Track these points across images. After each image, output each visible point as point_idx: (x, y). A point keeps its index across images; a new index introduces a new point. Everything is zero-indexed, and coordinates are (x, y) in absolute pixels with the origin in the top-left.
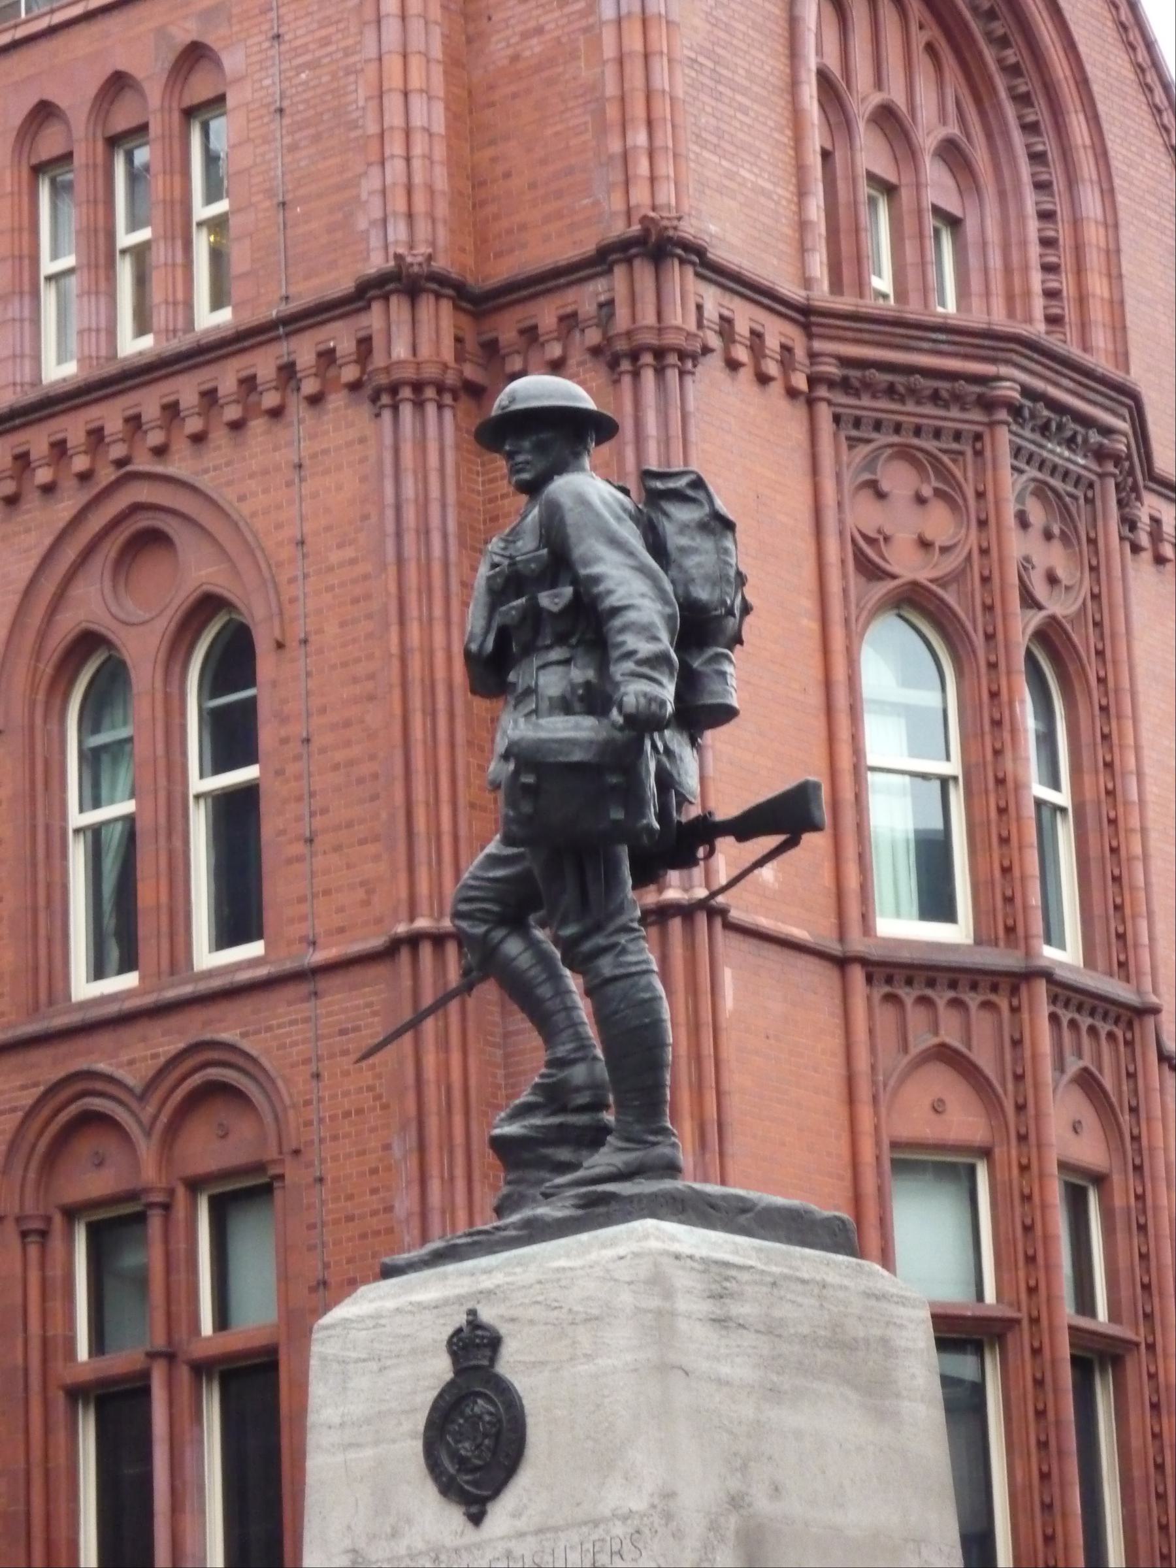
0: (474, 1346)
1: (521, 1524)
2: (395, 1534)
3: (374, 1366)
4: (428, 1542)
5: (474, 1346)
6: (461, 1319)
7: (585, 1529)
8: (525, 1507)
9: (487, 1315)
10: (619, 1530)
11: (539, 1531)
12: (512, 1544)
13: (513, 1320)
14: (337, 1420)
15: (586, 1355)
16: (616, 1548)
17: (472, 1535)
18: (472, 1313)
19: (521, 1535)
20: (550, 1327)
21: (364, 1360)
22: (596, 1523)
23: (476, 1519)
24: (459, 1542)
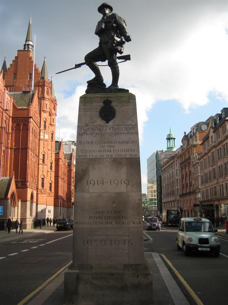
2: (93, 123)
3: (90, 103)
7: (125, 126)
8: (115, 122)
10: (130, 126)
11: (117, 125)
12: (113, 126)
14: (84, 108)
16: (130, 128)
17: (107, 124)
19: (114, 125)
22: (127, 125)
23: (108, 123)
24: (104, 125)
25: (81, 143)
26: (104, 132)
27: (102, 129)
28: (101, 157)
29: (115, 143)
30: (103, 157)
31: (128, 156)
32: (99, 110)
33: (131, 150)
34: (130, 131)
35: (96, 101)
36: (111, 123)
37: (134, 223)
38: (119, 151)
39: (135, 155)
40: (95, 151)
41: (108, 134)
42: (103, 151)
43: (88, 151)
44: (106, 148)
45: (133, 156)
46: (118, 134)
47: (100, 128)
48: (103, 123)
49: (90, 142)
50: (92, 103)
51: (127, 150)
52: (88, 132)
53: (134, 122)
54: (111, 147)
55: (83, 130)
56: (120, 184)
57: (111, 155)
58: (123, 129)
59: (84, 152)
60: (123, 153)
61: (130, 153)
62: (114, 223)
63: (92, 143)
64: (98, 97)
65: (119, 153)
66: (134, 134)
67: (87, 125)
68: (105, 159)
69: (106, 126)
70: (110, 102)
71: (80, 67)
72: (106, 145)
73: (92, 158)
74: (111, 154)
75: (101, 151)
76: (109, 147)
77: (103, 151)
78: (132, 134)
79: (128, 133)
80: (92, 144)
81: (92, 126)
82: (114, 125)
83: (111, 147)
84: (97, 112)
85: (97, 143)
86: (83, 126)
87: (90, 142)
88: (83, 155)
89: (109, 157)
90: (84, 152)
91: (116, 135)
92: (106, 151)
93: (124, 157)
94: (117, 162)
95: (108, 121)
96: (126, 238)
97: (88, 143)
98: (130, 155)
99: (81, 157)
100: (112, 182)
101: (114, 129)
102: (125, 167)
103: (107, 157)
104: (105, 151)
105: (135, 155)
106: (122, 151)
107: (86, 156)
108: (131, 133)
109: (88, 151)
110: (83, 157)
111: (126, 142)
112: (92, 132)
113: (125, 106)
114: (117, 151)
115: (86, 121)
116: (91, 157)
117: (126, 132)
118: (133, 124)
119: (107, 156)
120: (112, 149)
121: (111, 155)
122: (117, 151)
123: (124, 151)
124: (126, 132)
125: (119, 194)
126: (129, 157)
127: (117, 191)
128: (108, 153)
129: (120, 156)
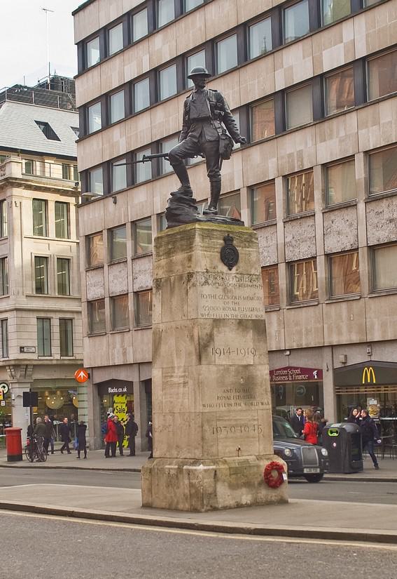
0: (228, 240)
9: (231, 235)
10: (254, 277)
23: (230, 270)
32: (219, 250)
34: (255, 283)
36: (234, 269)
37: (262, 404)
44: (231, 305)
48: (225, 269)
56: (247, 353)
59: (207, 309)
60: (249, 313)
61: (255, 313)
62: (242, 404)
63: (215, 297)
64: (217, 230)
67: (207, 272)
70: (232, 240)
72: (231, 301)
74: (236, 313)
82: (237, 274)
94: (242, 324)
96: (256, 423)
98: (256, 317)
100: (239, 352)
116: (215, 317)
117: (249, 283)
125: (246, 367)
127: (245, 363)
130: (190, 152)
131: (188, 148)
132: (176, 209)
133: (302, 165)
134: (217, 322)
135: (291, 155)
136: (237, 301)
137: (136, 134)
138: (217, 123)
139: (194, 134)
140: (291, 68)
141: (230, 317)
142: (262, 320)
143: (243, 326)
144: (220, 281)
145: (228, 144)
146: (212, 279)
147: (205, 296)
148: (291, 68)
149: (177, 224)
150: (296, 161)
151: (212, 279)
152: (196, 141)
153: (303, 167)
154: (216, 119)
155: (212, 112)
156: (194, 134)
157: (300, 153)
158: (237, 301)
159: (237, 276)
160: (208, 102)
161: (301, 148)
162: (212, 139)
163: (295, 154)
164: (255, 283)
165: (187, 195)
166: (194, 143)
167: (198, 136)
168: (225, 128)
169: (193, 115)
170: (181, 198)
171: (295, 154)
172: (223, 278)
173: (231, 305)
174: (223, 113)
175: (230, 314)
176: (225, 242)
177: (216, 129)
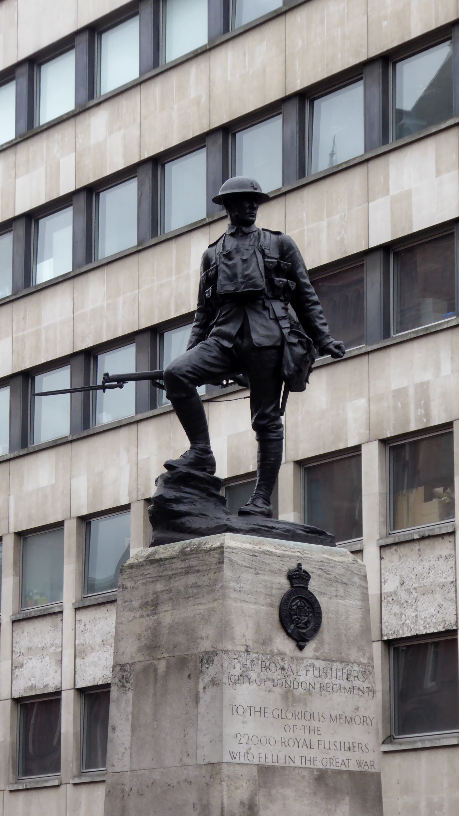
0: (298, 577)
1: (317, 654)
3: (253, 571)
4: (279, 651)
5: (298, 577)
6: (294, 566)
10: (356, 668)
12: (314, 661)
13: (313, 573)
15: (342, 596)
16: (356, 675)
17: (298, 654)
18: (299, 565)
20: (326, 580)
21: (249, 567)
23: (301, 648)
25: (235, 708)
26: (291, 679)
27: (286, 666)
28: (287, 765)
29: (322, 719)
30: (292, 764)
31: (353, 767)
33: (360, 746)
35: (267, 568)
38: (333, 747)
39: (369, 764)
40: (272, 742)
41: (304, 685)
42: (291, 743)
43: (255, 739)
44: (301, 735)
45: (366, 768)
46: (329, 690)
47: (282, 664)
49: (258, 709)
50: (257, 574)
51: (351, 746)
52: (253, 675)
53: (364, 654)
54: (312, 732)
55: (238, 666)
57: (312, 760)
58: (339, 674)
59: (244, 740)
60: (341, 756)
64: (271, 554)
65: (332, 753)
66: (366, 694)
68: (297, 771)
69: (297, 659)
71: (121, 387)
72: (300, 723)
73: (264, 763)
74: (312, 753)
75: (286, 743)
76: (307, 731)
77: (291, 743)
78: (360, 692)
79: (352, 690)
80: (263, 715)
81: (263, 654)
82: (318, 658)
83: (312, 732)
84: (271, 605)
85: (276, 715)
86: (239, 652)
87: (258, 709)
88: (242, 754)
89: (308, 765)
90: (244, 740)
91: (323, 692)
92: (300, 745)
93: (343, 768)
95: (302, 644)
97: (253, 712)
98: (359, 764)
99: (237, 760)
101: (317, 673)
102: (347, 800)
103: (304, 765)
104: (296, 743)
105: (369, 764)
106: (339, 748)
107: (250, 757)
108: (359, 689)
109: (255, 739)
110: (242, 760)
111: (349, 719)
112: (263, 676)
113: (343, 598)
114: (327, 746)
115: (244, 636)
116: (262, 761)
117: (348, 685)
118: (362, 662)
119: (304, 761)
120: (315, 739)
121: (312, 760)
122: (327, 746)
123: (343, 749)
124: (348, 685)
126: (357, 769)
128: (305, 751)
129: (334, 763)
130: (213, 369)
131: (210, 360)
132: (177, 501)
133: (427, 414)
134: (267, 774)
135: (400, 394)
136: (315, 724)
137: (38, 334)
138: (278, 307)
139: (225, 328)
140: (407, 196)
141: (298, 763)
142: (372, 774)
143: (327, 785)
144: (277, 675)
145: (305, 355)
146: (257, 669)
147: (240, 711)
148: (407, 196)
149: (181, 535)
150: (412, 407)
151: (257, 669)
152: (230, 346)
153: (428, 421)
154: (276, 298)
155: (270, 282)
156: (225, 328)
157: (423, 389)
158: (315, 724)
159: (318, 664)
160: (259, 256)
161: (427, 376)
162: (266, 343)
163: (411, 391)
164: (357, 683)
165: (204, 470)
166: (223, 349)
167: (234, 332)
168: (296, 319)
169: (225, 286)
170: (189, 474)
171: (411, 391)
172: (283, 669)
173: (301, 735)
174: (293, 285)
175: (298, 756)
176: (292, 584)
177: (277, 320)
